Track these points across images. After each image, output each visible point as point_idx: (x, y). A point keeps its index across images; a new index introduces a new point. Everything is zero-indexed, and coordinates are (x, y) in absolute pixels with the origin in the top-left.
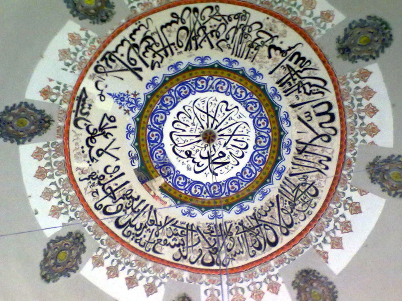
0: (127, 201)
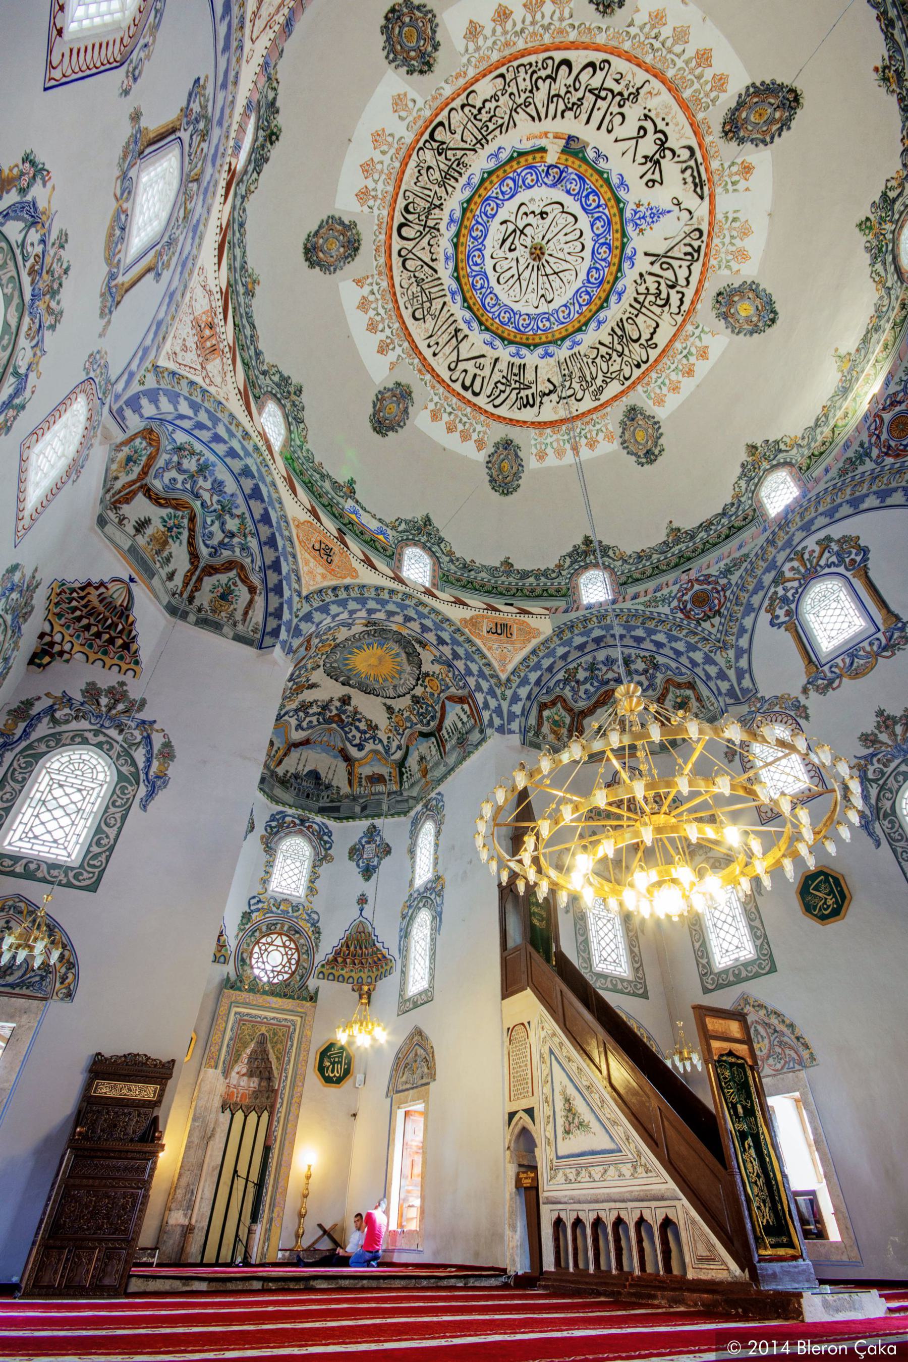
0: (574, 100)
